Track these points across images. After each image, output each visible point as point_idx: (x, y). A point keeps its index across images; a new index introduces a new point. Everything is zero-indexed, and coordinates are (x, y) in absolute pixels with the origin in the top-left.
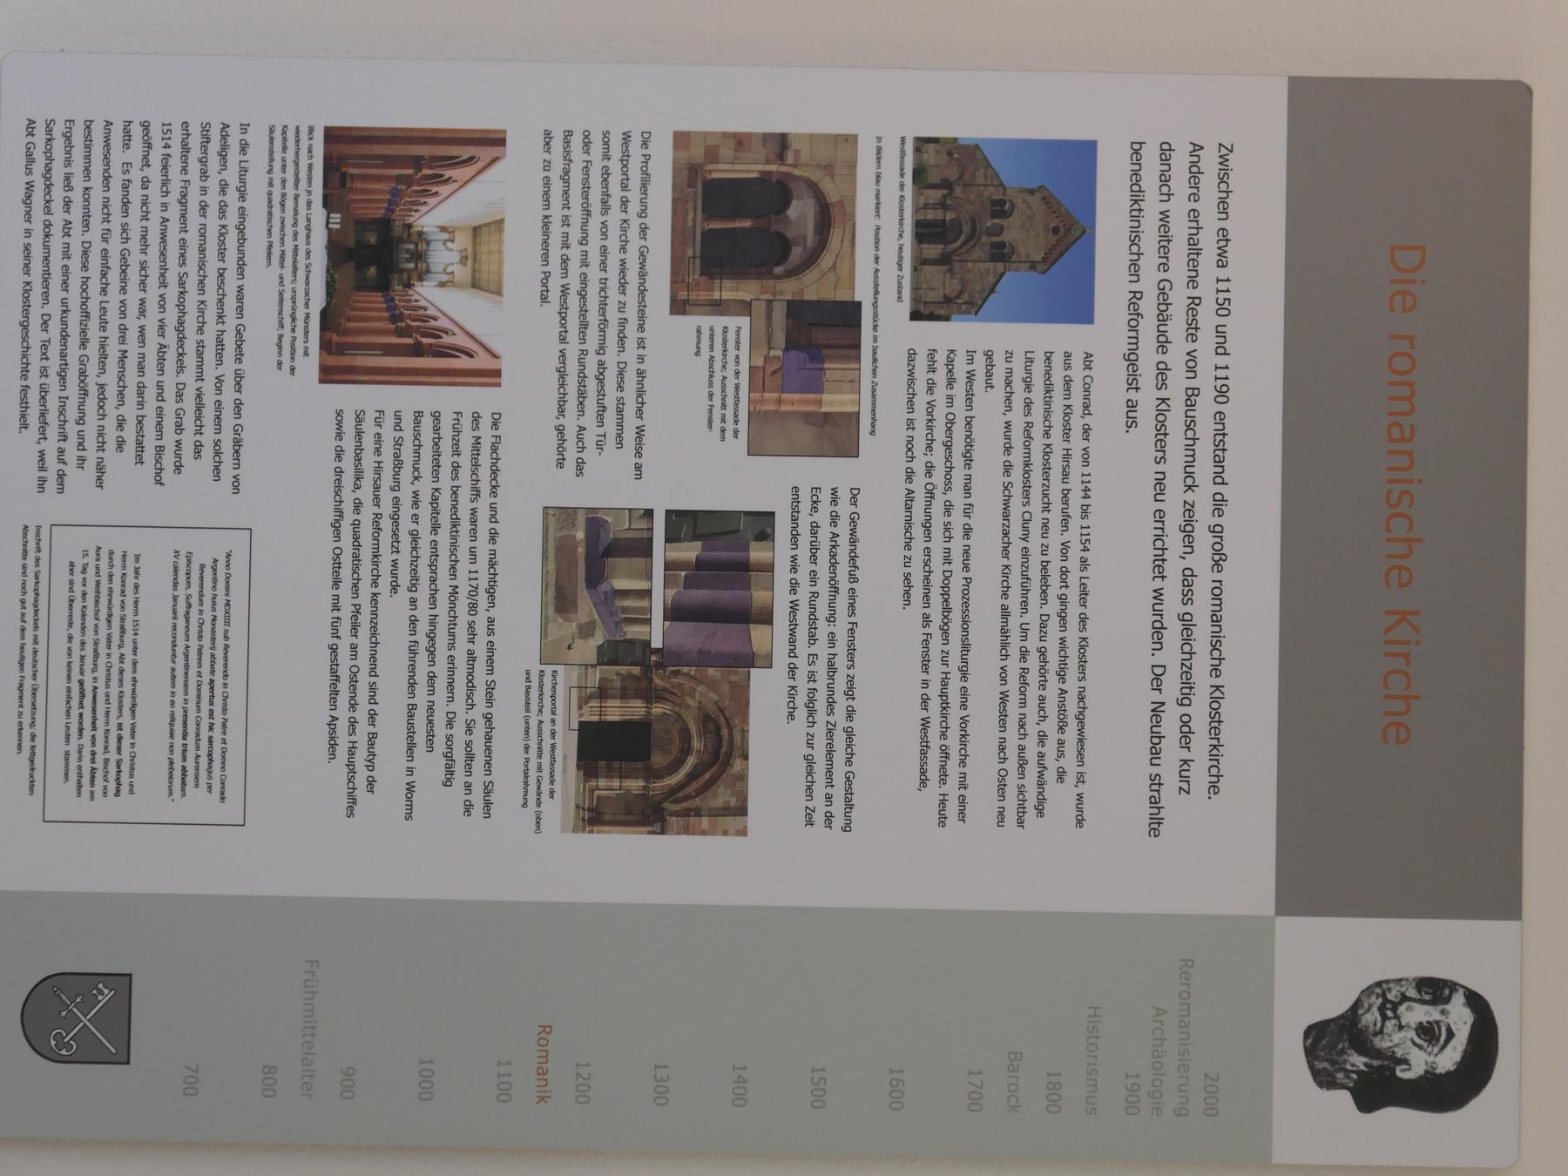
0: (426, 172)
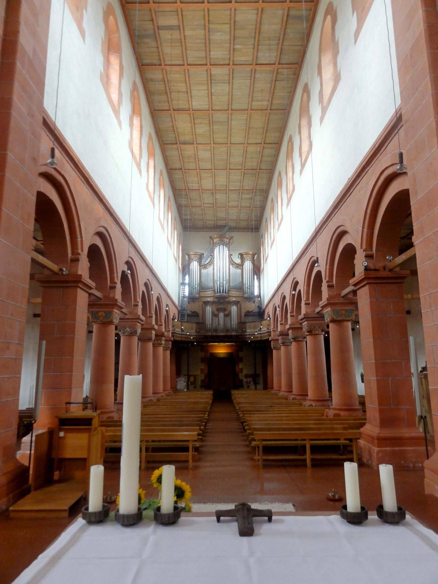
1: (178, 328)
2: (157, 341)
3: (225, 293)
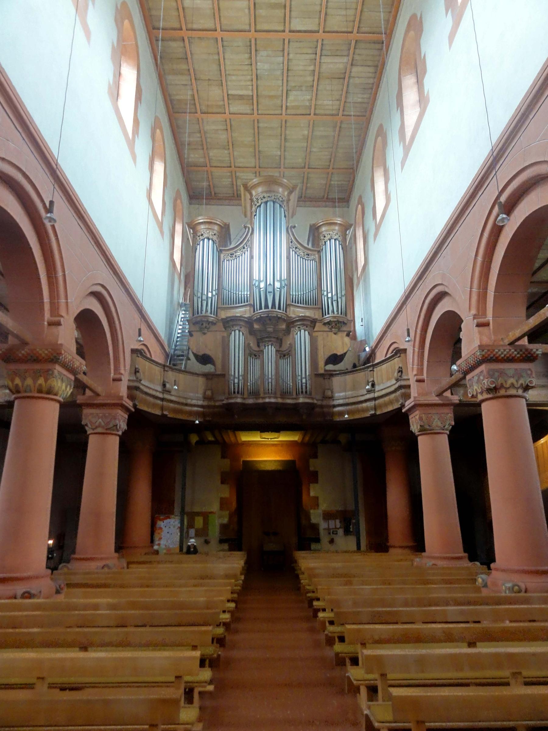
1: (151, 381)
2: (35, 380)
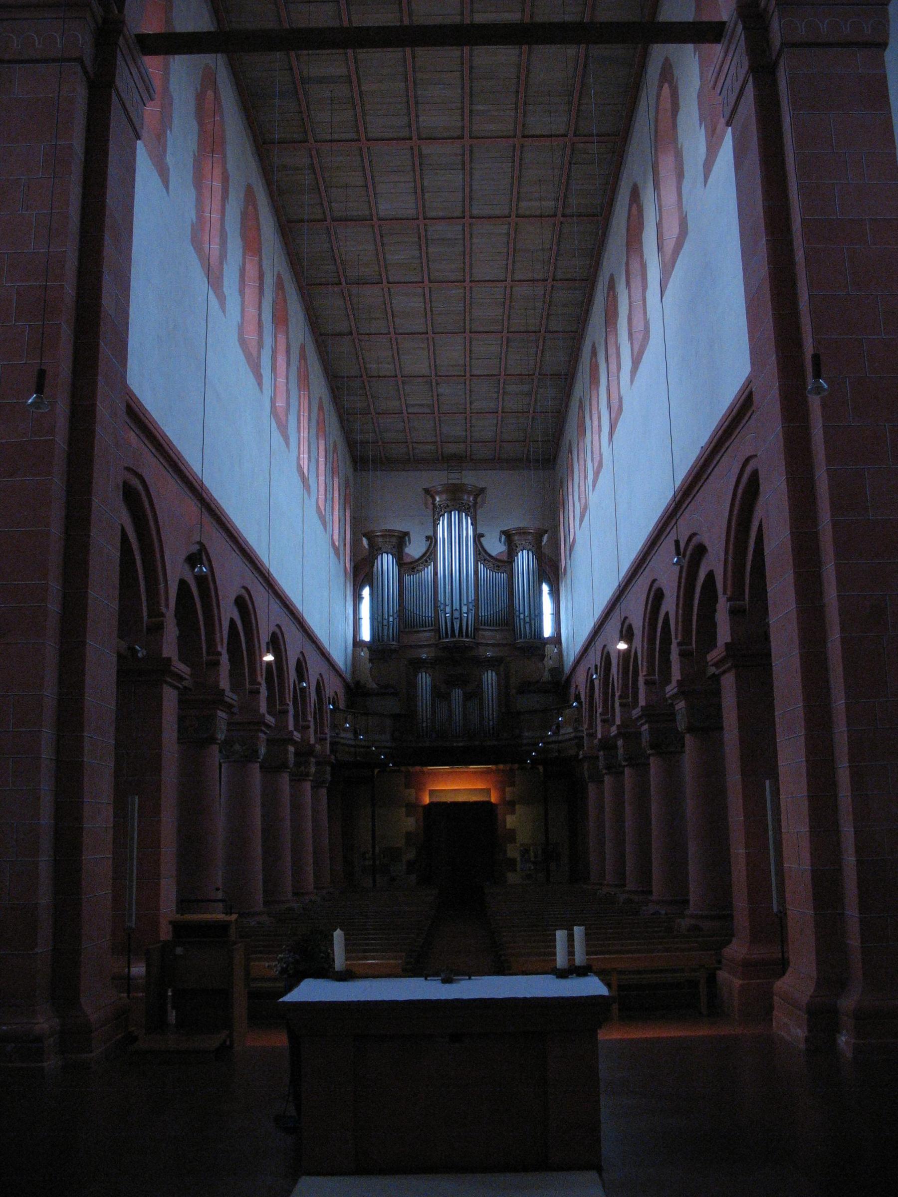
0: (170, 648)
3: (467, 636)
